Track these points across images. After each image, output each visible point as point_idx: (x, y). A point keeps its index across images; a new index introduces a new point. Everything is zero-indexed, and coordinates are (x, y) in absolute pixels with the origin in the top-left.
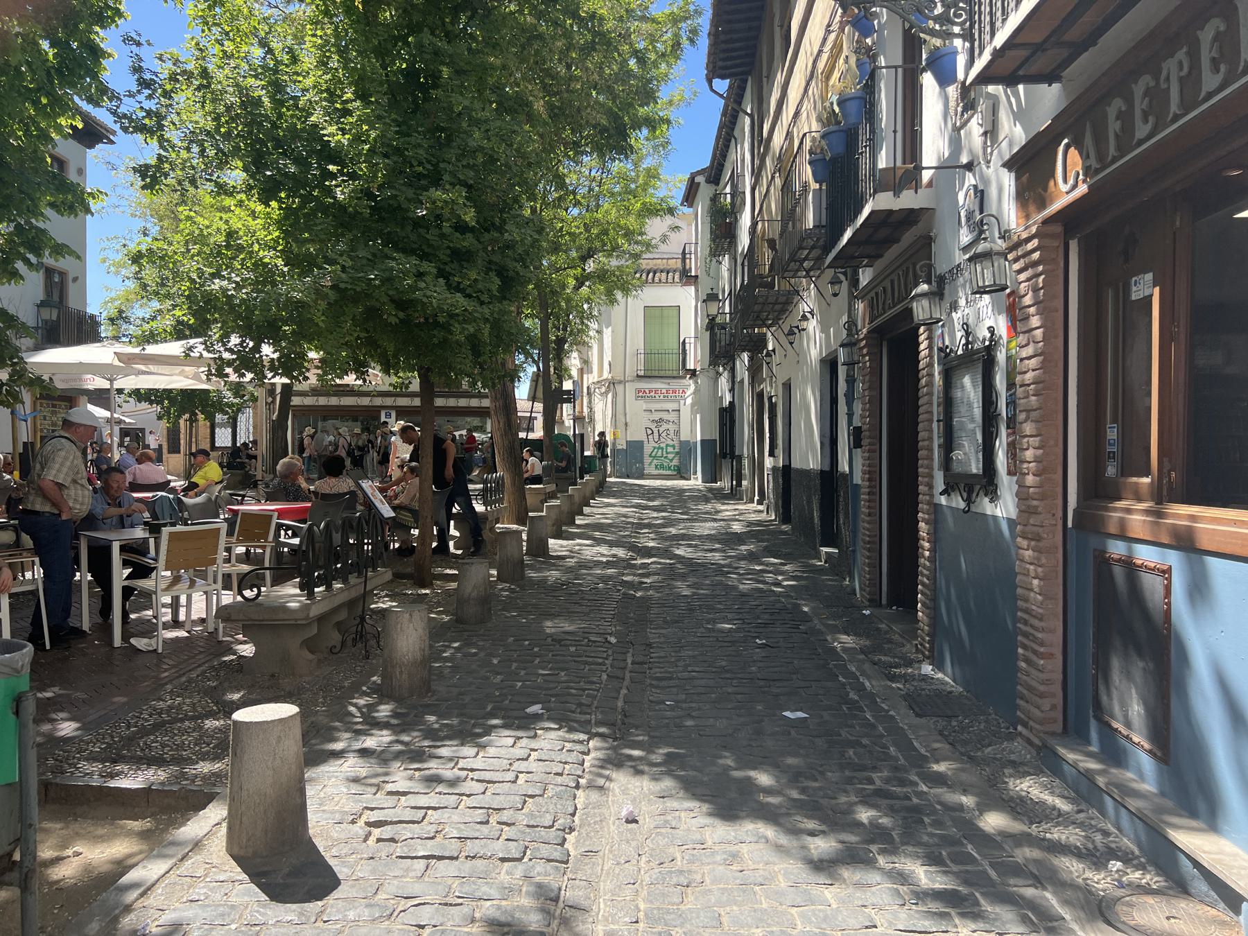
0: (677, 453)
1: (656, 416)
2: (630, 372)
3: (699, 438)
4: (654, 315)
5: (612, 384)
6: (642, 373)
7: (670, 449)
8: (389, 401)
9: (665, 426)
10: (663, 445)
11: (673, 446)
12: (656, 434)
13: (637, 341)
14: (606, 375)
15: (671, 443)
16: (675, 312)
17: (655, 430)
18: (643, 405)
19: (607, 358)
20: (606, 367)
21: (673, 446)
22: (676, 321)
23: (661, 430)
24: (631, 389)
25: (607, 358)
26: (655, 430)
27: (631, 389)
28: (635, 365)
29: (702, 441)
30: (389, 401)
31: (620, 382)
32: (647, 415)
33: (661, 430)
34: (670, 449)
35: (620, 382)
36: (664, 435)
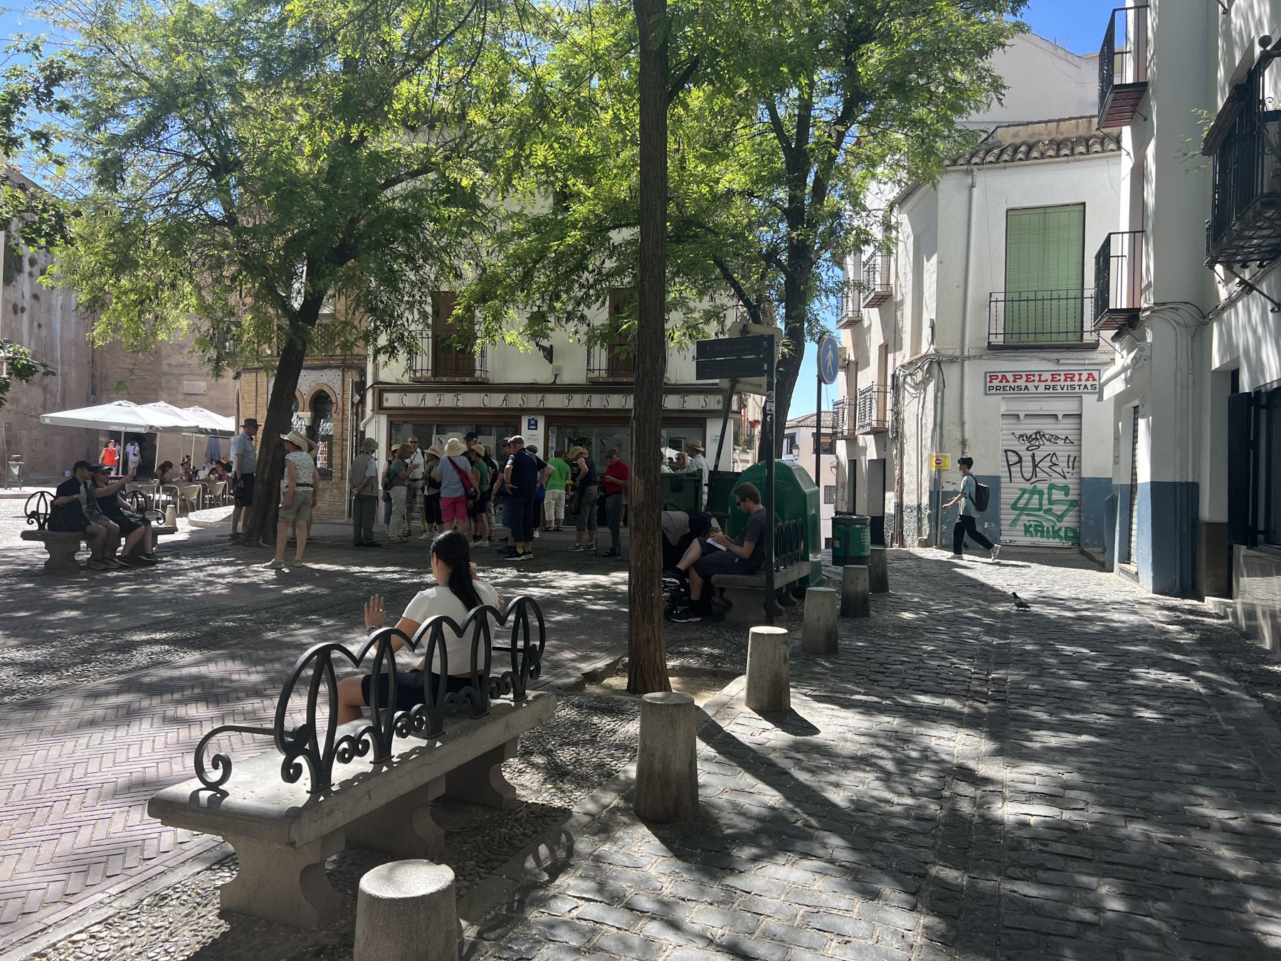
0: (1073, 504)
1: (1030, 427)
2: (975, 338)
3: (1144, 475)
4: (1026, 225)
5: (936, 363)
6: (999, 340)
7: (1058, 495)
8: (533, 401)
9: (1047, 448)
10: (1039, 486)
11: (1066, 489)
12: (1027, 463)
13: (990, 276)
14: (926, 348)
15: (1060, 481)
16: (1076, 216)
17: (1027, 457)
18: (1002, 405)
19: (929, 314)
20: (926, 332)
21: (1066, 489)
22: (1076, 234)
23: (1039, 454)
24: (974, 374)
25: (929, 314)
26: (1027, 457)
27: (974, 374)
28: (986, 324)
29: (1156, 486)
30: (533, 401)
31: (953, 360)
32: (1010, 425)
33: (1039, 454)
34: (1058, 495)
35: (953, 360)
36: (1045, 465)
